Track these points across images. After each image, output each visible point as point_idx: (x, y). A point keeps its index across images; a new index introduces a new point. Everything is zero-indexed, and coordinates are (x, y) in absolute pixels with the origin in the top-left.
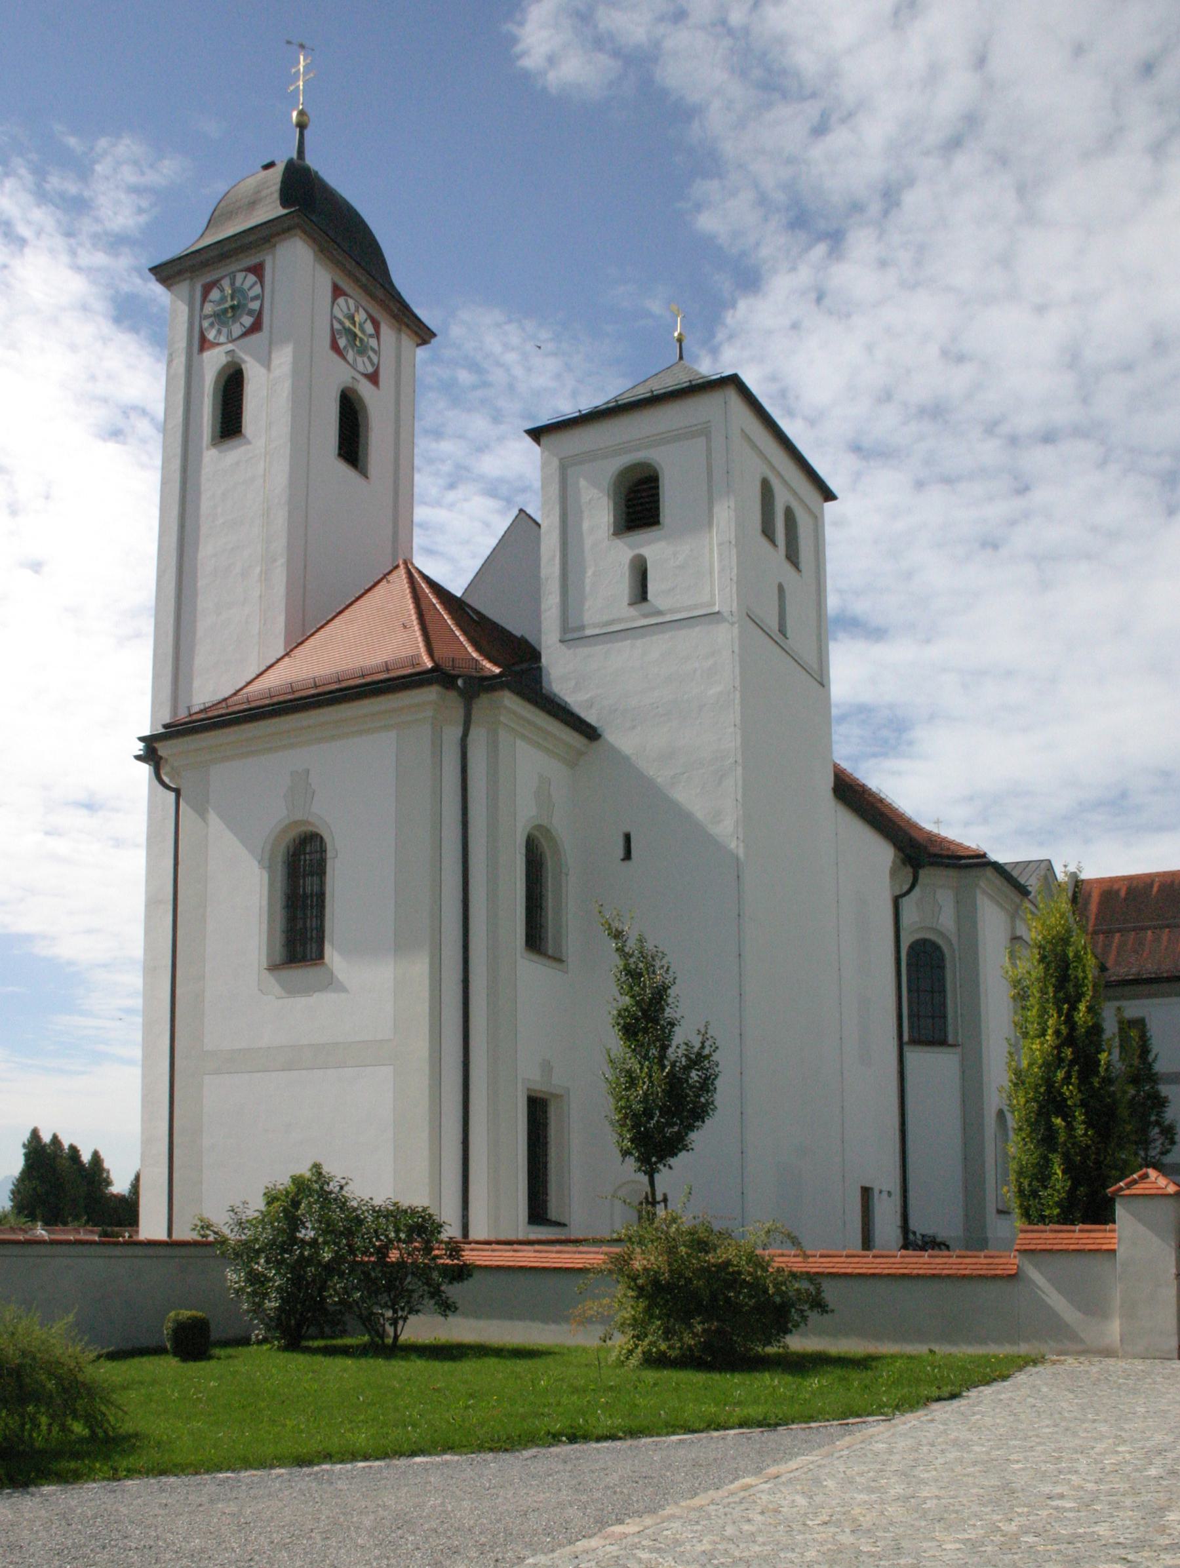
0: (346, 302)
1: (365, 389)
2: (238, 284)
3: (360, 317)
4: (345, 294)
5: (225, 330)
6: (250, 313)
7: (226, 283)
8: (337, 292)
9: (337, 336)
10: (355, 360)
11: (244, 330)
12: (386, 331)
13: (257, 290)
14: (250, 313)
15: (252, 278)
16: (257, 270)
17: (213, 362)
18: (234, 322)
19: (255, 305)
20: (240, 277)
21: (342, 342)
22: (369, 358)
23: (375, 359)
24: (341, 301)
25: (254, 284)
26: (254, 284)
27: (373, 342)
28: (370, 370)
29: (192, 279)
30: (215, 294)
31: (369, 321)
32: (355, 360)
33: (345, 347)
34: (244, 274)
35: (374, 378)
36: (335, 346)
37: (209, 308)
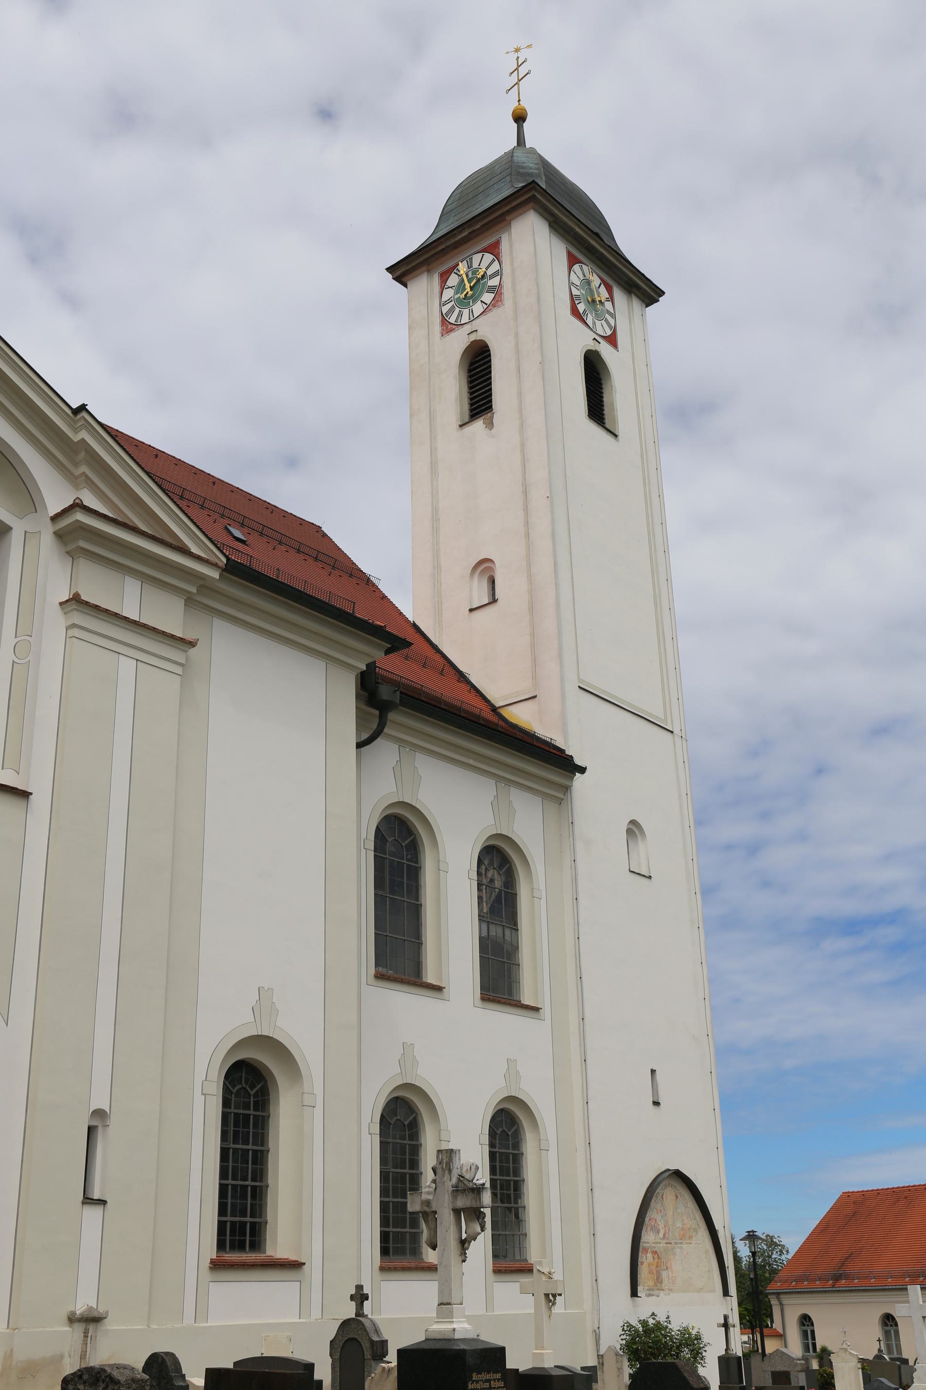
0: (582, 269)
1: (605, 350)
2: (475, 265)
3: (596, 281)
4: (579, 262)
5: (466, 312)
6: (491, 289)
7: (463, 268)
8: (572, 261)
9: (577, 302)
10: (594, 323)
11: (485, 306)
12: (618, 294)
13: (495, 267)
14: (491, 289)
15: (488, 257)
16: (494, 249)
17: (459, 342)
18: (474, 302)
19: (494, 282)
20: (476, 258)
21: (581, 308)
22: (606, 321)
23: (612, 322)
24: (576, 267)
25: (493, 261)
26: (493, 261)
27: (608, 305)
28: (609, 332)
29: (428, 271)
30: (453, 280)
31: (602, 285)
32: (594, 323)
33: (585, 311)
34: (481, 254)
35: (612, 340)
36: (575, 312)
37: (448, 294)
